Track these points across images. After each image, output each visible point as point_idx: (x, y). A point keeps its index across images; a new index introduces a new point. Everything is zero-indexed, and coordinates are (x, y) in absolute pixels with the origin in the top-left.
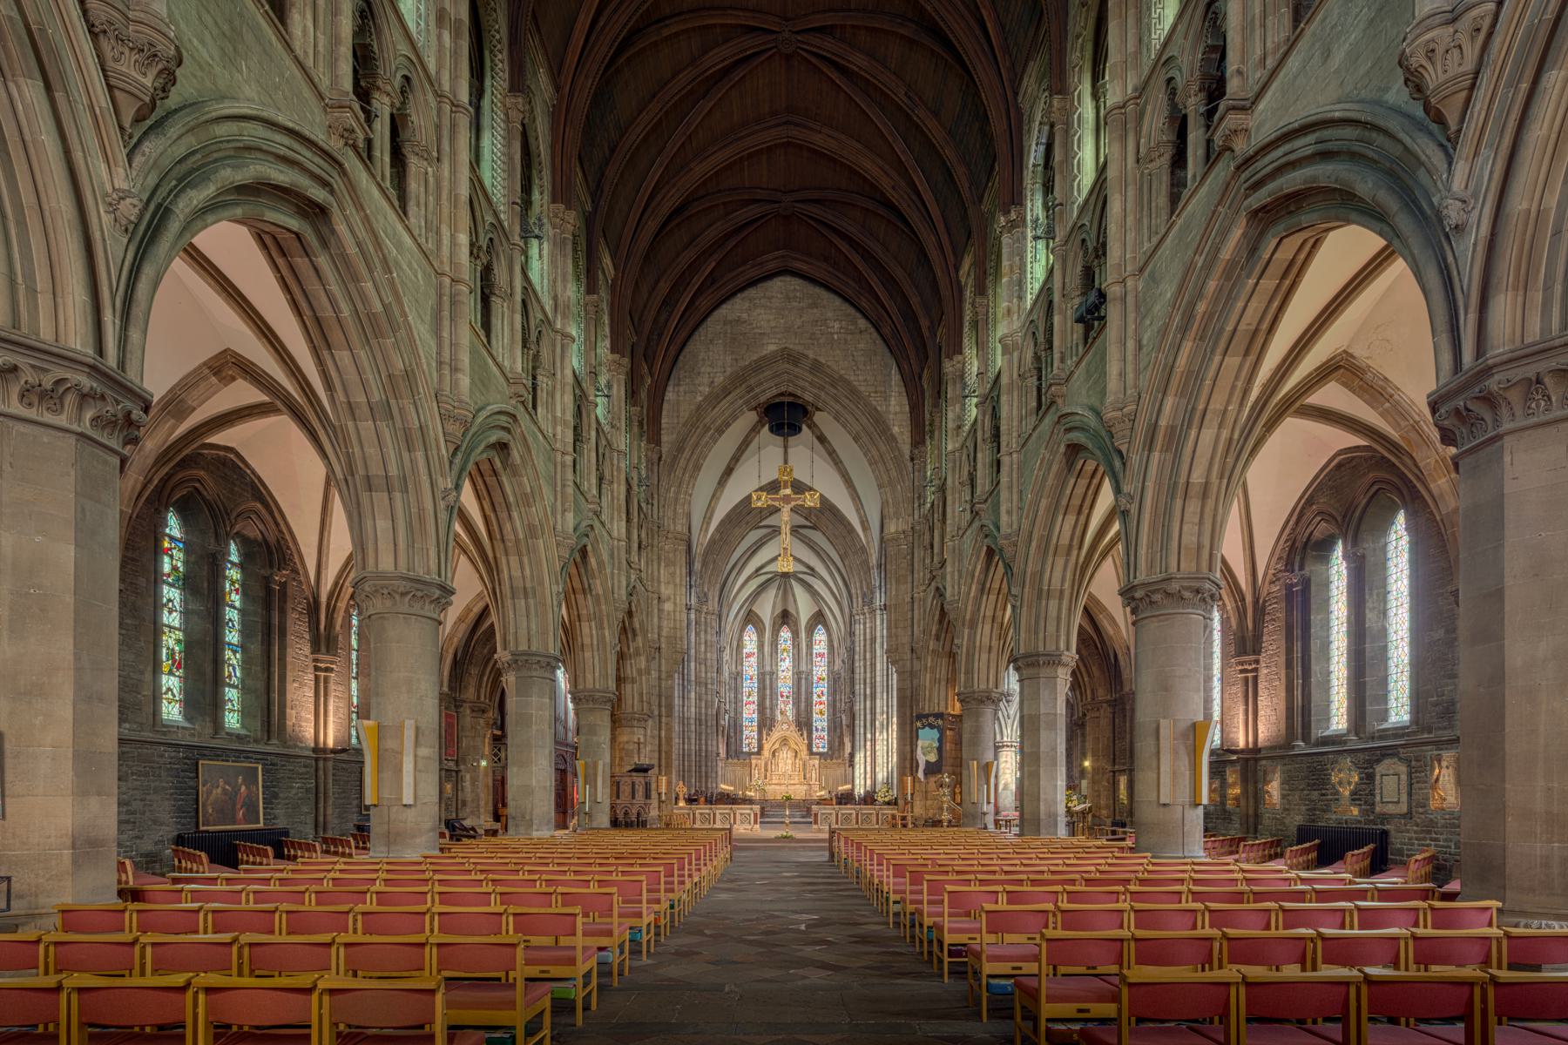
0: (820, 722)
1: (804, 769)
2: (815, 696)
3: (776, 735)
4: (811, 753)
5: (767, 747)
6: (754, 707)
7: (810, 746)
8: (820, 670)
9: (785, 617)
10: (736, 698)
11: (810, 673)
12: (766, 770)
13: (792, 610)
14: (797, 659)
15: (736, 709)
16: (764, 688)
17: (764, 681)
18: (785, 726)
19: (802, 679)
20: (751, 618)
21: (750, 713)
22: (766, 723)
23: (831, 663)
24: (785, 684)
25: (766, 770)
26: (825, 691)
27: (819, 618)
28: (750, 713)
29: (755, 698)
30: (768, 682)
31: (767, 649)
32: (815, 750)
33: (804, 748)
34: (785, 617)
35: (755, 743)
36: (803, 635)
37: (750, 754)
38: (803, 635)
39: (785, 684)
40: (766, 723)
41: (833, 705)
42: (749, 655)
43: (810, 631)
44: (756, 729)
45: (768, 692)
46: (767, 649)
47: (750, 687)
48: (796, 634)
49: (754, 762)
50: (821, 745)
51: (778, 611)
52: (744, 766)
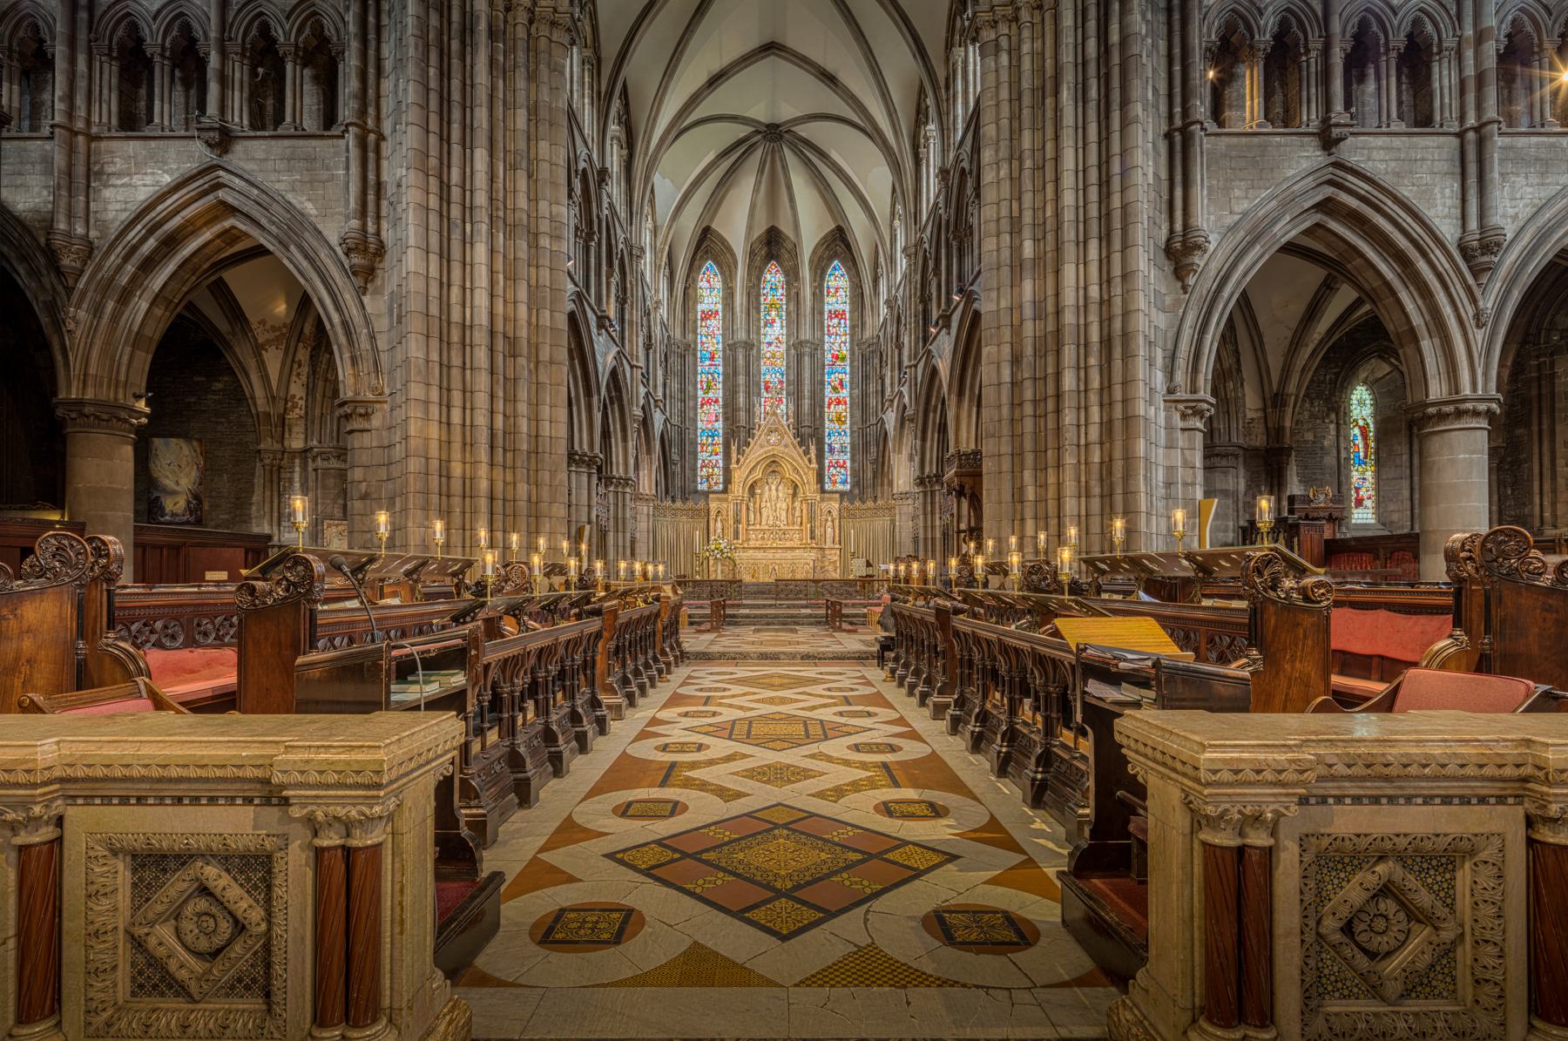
0: (839, 435)
1: (812, 519)
2: (828, 390)
3: (757, 452)
4: (823, 491)
5: (738, 476)
6: (717, 409)
7: (820, 479)
8: (838, 341)
9: (773, 245)
10: (683, 390)
11: (818, 346)
12: (737, 521)
13: (786, 228)
14: (794, 321)
15: (683, 413)
16: (735, 373)
17: (735, 360)
18: (773, 438)
19: (804, 353)
20: (707, 244)
21: (709, 420)
22: (738, 432)
23: (858, 325)
24: (773, 367)
25: (737, 521)
26: (847, 378)
27: (838, 243)
28: (709, 420)
29: (718, 393)
30: (741, 361)
31: (739, 299)
32: (828, 487)
33: (812, 477)
34: (773, 245)
35: (718, 473)
36: (806, 272)
37: (706, 494)
38: (806, 272)
39: (773, 367)
40: (738, 432)
41: (861, 405)
42: (707, 316)
43: (820, 270)
44: (720, 449)
45: (741, 379)
46: (739, 299)
47: (709, 376)
48: (792, 275)
49: (713, 506)
50: (840, 478)
51: (760, 230)
52: (694, 514)
